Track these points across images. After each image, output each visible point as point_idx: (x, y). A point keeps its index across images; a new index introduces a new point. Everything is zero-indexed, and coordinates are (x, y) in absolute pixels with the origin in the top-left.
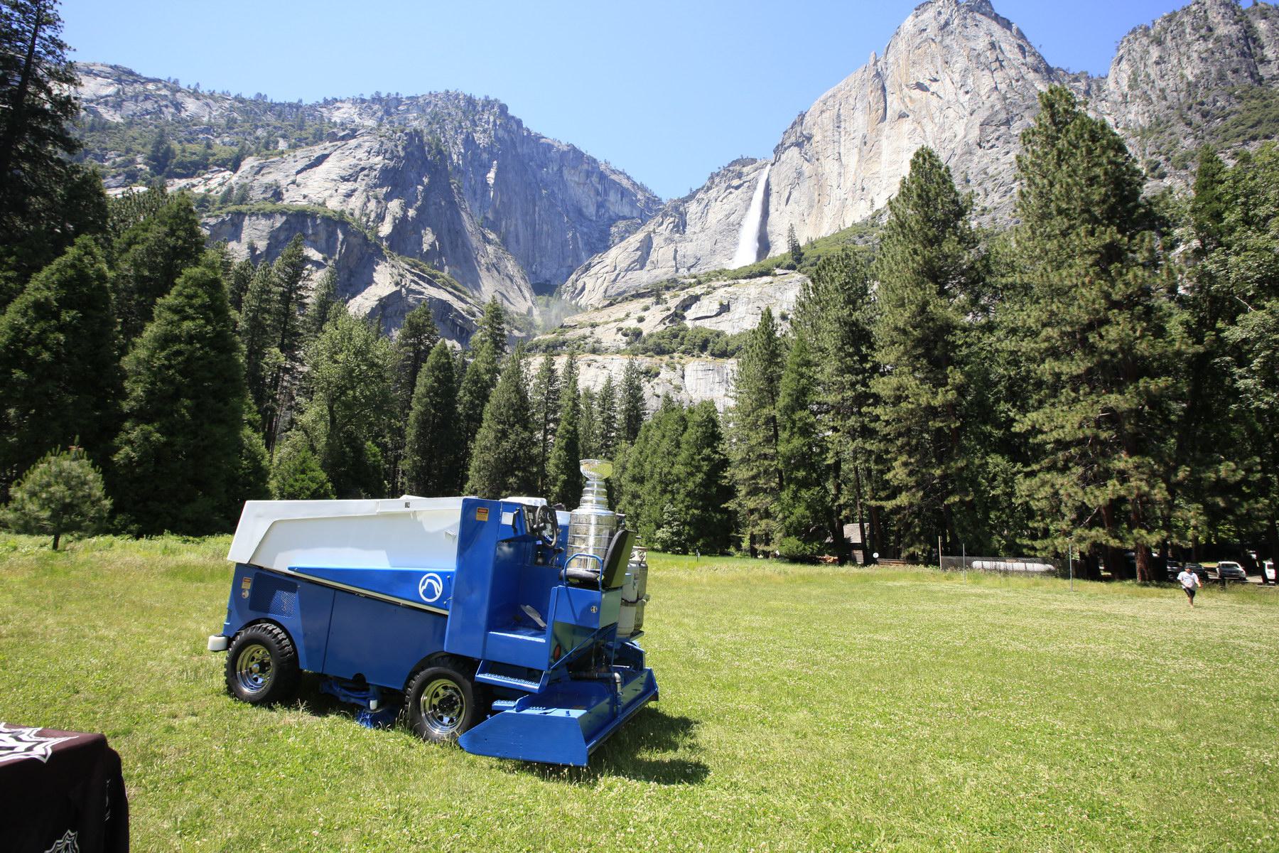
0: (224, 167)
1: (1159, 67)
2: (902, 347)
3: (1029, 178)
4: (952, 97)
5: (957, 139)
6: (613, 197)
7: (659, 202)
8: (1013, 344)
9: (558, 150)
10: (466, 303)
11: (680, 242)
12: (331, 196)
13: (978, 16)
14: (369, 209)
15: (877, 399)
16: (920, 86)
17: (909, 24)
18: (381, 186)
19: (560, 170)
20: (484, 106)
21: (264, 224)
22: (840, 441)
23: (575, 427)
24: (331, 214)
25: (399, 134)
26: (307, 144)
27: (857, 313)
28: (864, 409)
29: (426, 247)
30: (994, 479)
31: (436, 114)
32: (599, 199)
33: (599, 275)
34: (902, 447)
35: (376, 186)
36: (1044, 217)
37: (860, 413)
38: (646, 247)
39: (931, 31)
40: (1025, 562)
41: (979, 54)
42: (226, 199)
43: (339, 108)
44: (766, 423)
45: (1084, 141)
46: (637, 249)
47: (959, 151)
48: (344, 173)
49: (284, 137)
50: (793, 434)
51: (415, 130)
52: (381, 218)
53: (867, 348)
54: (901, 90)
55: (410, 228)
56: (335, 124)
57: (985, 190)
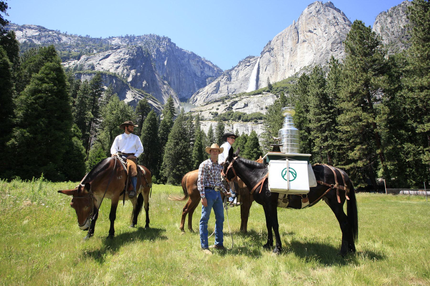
0: (75, 58)
1: (391, 24)
4: (321, 35)
5: (323, 49)
10: (157, 104)
12: (111, 68)
13: (329, 8)
16: (310, 31)
17: (306, 11)
18: (128, 65)
20: (163, 39)
21: (88, 78)
25: (134, 48)
26: (103, 51)
29: (144, 85)
31: (147, 42)
35: (126, 65)
43: (114, 40)
47: (324, 53)
48: (116, 61)
49: (95, 49)
51: (140, 46)
52: (128, 76)
54: (304, 33)
55: (138, 79)
56: (113, 45)
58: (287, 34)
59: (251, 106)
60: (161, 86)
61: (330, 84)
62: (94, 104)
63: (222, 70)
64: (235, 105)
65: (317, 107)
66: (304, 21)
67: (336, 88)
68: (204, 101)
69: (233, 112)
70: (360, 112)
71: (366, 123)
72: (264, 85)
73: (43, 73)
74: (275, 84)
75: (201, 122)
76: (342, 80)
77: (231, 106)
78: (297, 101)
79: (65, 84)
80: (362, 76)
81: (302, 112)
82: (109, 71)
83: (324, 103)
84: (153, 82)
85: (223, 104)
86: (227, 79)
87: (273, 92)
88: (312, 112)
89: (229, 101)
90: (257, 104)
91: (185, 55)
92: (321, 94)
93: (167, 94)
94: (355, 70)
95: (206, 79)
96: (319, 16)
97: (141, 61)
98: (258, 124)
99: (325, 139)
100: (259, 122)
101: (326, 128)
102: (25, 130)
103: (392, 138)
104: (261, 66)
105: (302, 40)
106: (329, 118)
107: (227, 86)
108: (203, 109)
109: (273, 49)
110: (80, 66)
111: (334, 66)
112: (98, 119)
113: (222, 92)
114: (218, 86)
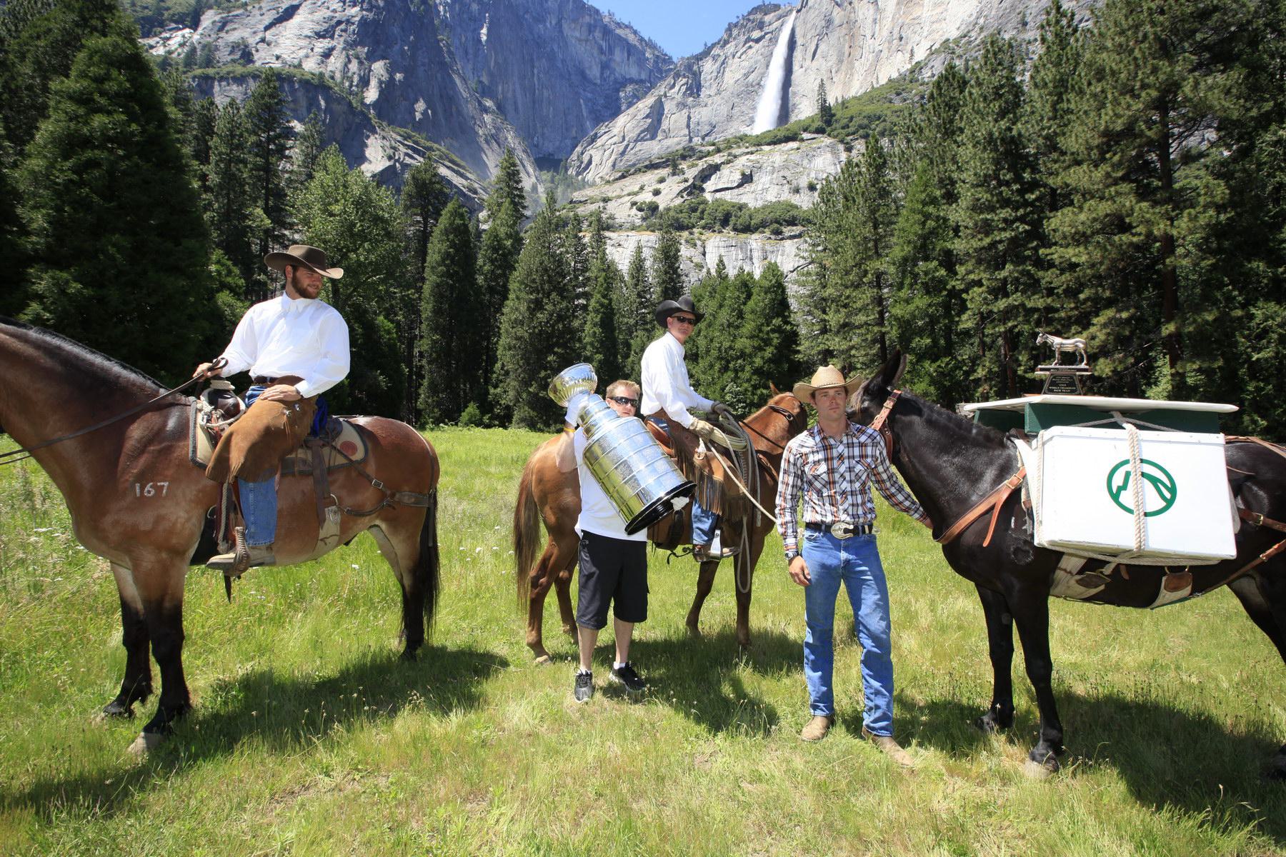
6: (618, 55)
7: (668, 60)
10: (467, 178)
11: (694, 107)
12: (307, 56)
14: (351, 71)
18: (362, 44)
19: (559, 24)
21: (235, 91)
24: (309, 77)
32: (604, 58)
33: (606, 147)
38: (657, 113)
42: (190, 60)
46: (647, 117)
48: (318, 28)
52: (365, 82)
55: (398, 93)
59: (762, 180)
60: (473, 117)
61: (1037, 101)
62: (268, 182)
65: (982, 185)
67: (1055, 118)
69: (705, 202)
70: (1128, 201)
71: (1142, 238)
73: (83, 75)
74: (843, 103)
75: (607, 234)
76: (1080, 88)
78: (919, 164)
79: (166, 114)
80: (1155, 70)
81: (933, 201)
82: (300, 65)
83: (1009, 170)
84: (446, 102)
85: (674, 174)
87: (835, 133)
88: (963, 203)
89: (693, 166)
91: (546, 6)
92: (1003, 140)
93: (495, 145)
94: (1132, 51)
95: (618, 91)
97: (403, 29)
98: (782, 239)
99: (1000, 291)
100: (787, 234)
101: (1005, 252)
102: (65, 275)
103: (1221, 285)
106: (1022, 220)
107: (685, 112)
108: (611, 191)
110: (203, 50)
111: (1057, 35)
112: (287, 232)
113: (672, 135)
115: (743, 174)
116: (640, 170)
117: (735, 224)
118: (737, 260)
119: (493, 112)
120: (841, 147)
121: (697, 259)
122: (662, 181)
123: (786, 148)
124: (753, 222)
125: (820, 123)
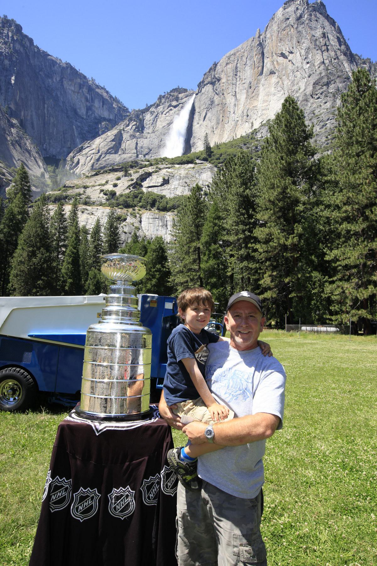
2: (272, 212)
3: (343, 122)
4: (300, 65)
8: (328, 213)
9: (60, 66)
15: (256, 240)
22: (235, 262)
23: (78, 251)
27: (248, 191)
28: (250, 245)
30: (314, 285)
34: (269, 266)
36: (349, 145)
37: (246, 247)
39: (292, 20)
40: (326, 327)
41: (316, 40)
44: (195, 251)
45: (373, 104)
47: (301, 99)
50: (209, 257)
53: (253, 211)
54: (273, 56)
57: (313, 123)
58: (246, 54)
59: (174, 183)
60: (4, 130)
63: (127, 109)
64: (148, 179)
66: (275, 34)
68: (93, 166)
69: (142, 193)
72: (199, 147)
77: (139, 182)
85: (125, 176)
86: (136, 128)
89: (137, 172)
90: (184, 180)
96: (300, 28)
104: (197, 110)
105: (268, 70)
109: (219, 80)
114: (118, 139)
115: (164, 179)
116: (106, 171)
117: (158, 206)
118: (158, 226)
119: (18, 127)
120: (216, 169)
121: (136, 225)
122: (119, 179)
123: (187, 167)
124: (168, 206)
125: (205, 155)
